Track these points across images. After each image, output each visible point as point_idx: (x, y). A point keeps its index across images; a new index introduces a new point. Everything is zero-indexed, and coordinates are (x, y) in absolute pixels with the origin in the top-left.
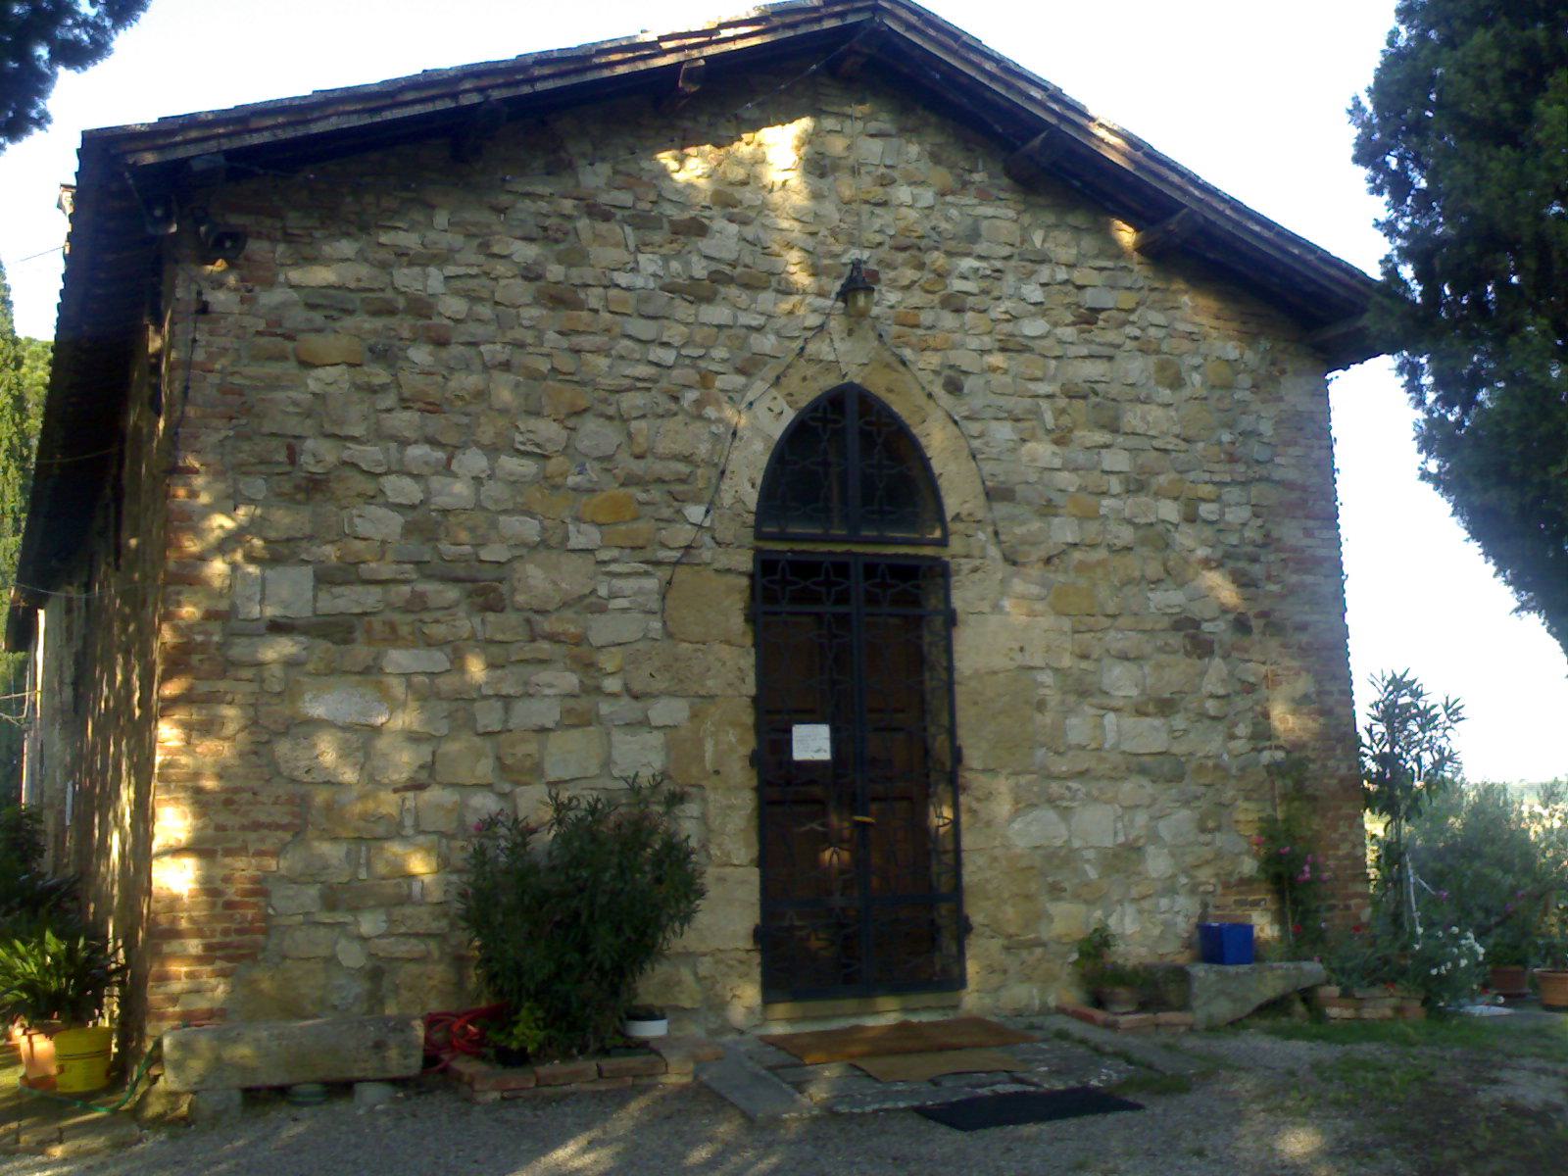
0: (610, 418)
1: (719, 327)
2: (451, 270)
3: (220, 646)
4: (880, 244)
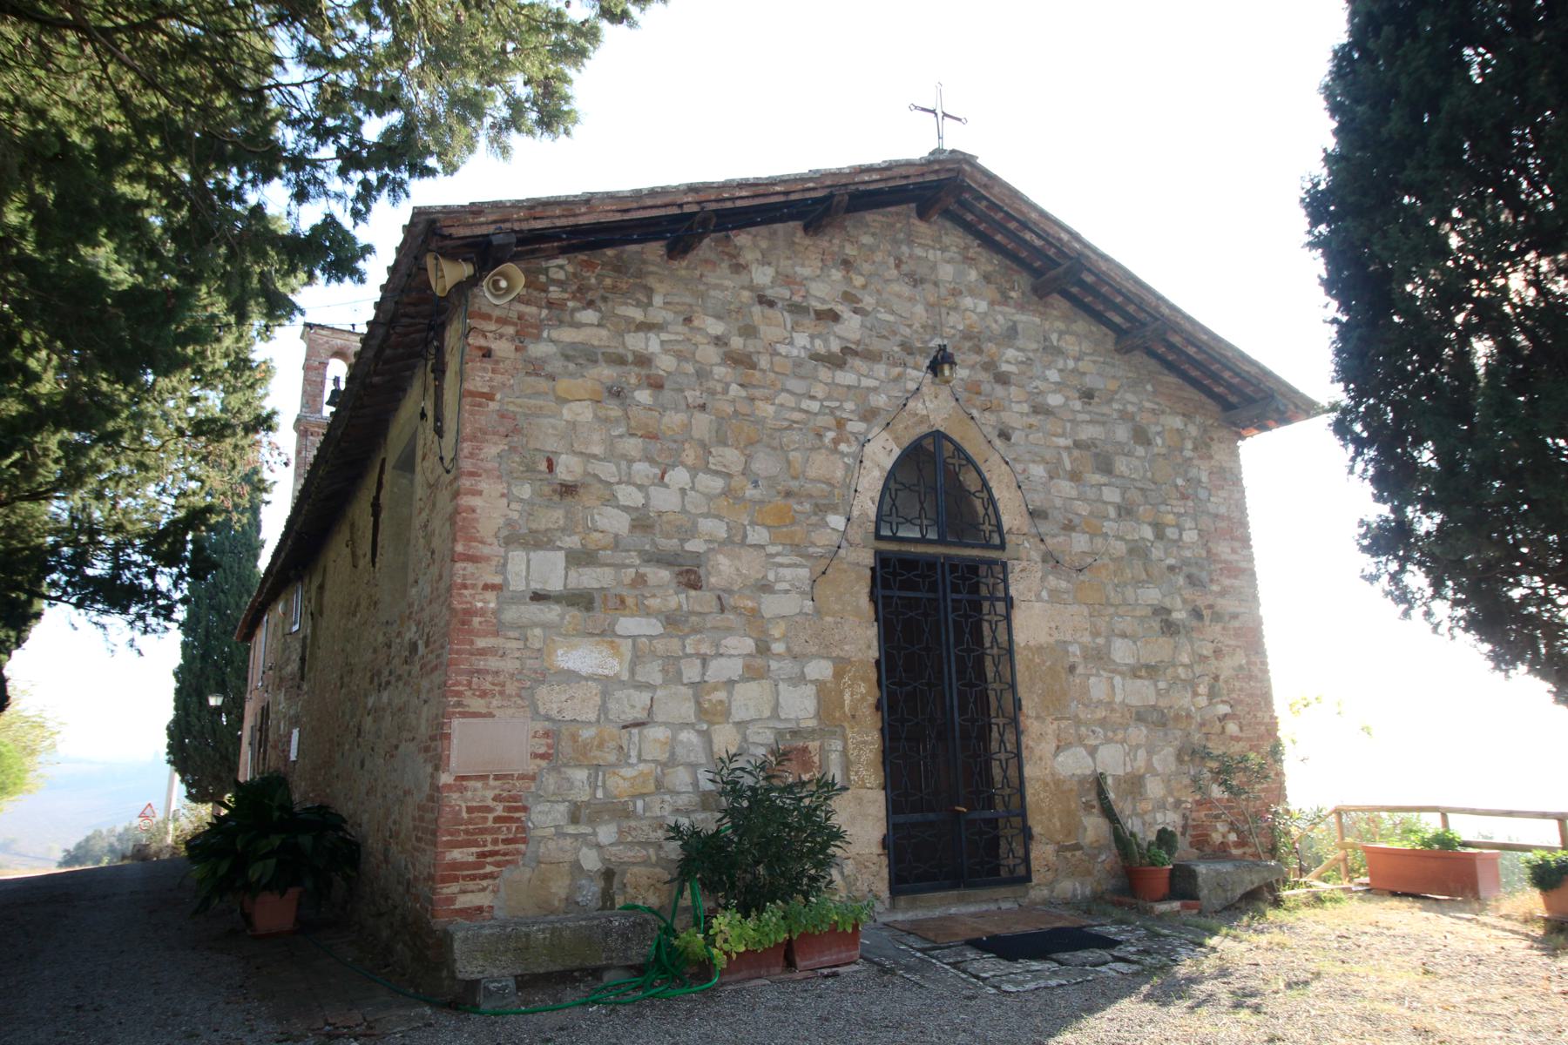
0: (774, 449)
1: (849, 387)
2: (664, 336)
3: (495, 613)
4: (954, 335)
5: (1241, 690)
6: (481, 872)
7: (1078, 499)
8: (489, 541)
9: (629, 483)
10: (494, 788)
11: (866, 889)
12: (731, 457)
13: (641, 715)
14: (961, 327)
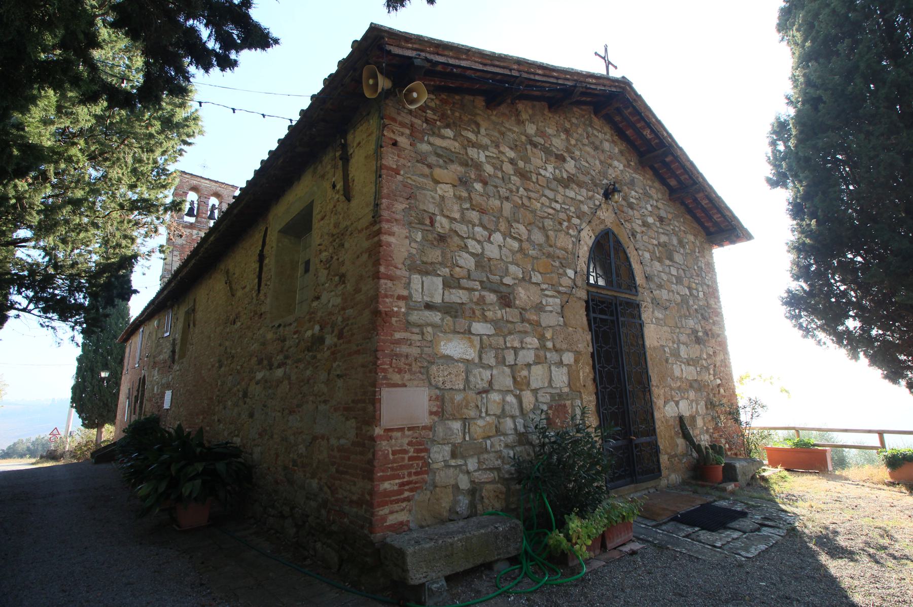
1: (571, 198)
2: (487, 153)
3: (406, 314)
6: (402, 497)
10: (408, 436)
13: (486, 385)
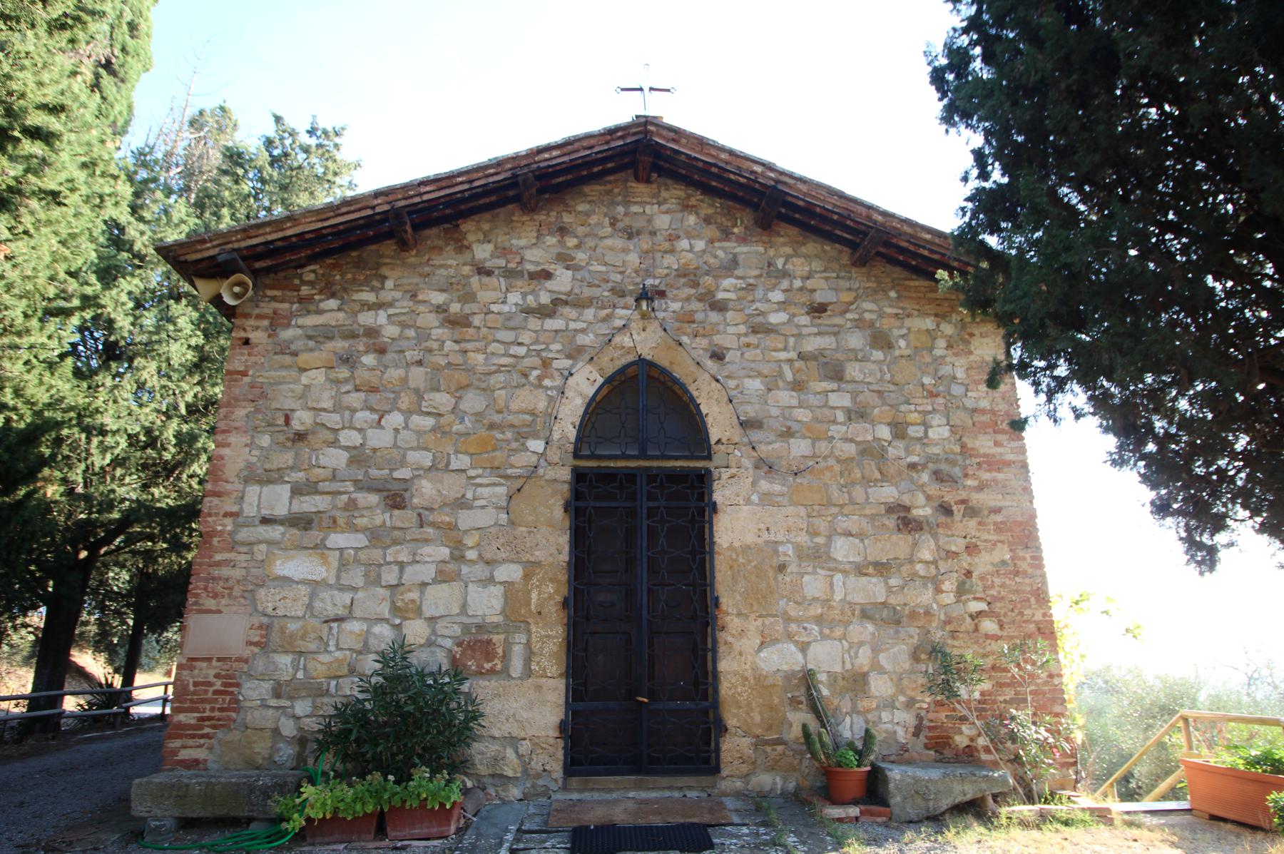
0: (484, 390)
1: (556, 331)
2: (391, 311)
3: (230, 533)
4: (667, 275)
5: (1003, 586)
6: (200, 732)
7: (800, 407)
8: (231, 480)
9: (351, 428)
10: (215, 668)
11: (540, 768)
12: (442, 400)
13: (341, 612)
14: (676, 267)
